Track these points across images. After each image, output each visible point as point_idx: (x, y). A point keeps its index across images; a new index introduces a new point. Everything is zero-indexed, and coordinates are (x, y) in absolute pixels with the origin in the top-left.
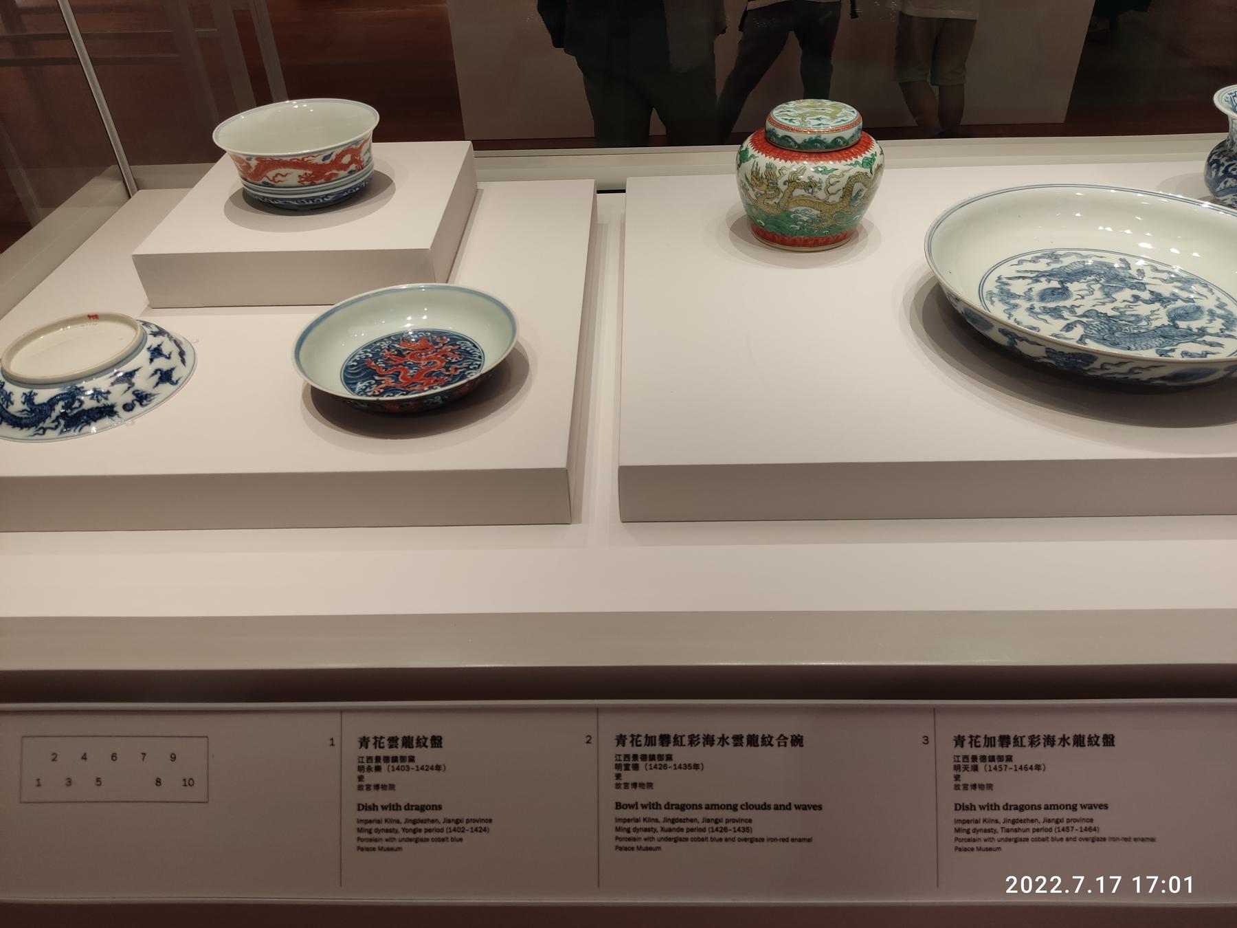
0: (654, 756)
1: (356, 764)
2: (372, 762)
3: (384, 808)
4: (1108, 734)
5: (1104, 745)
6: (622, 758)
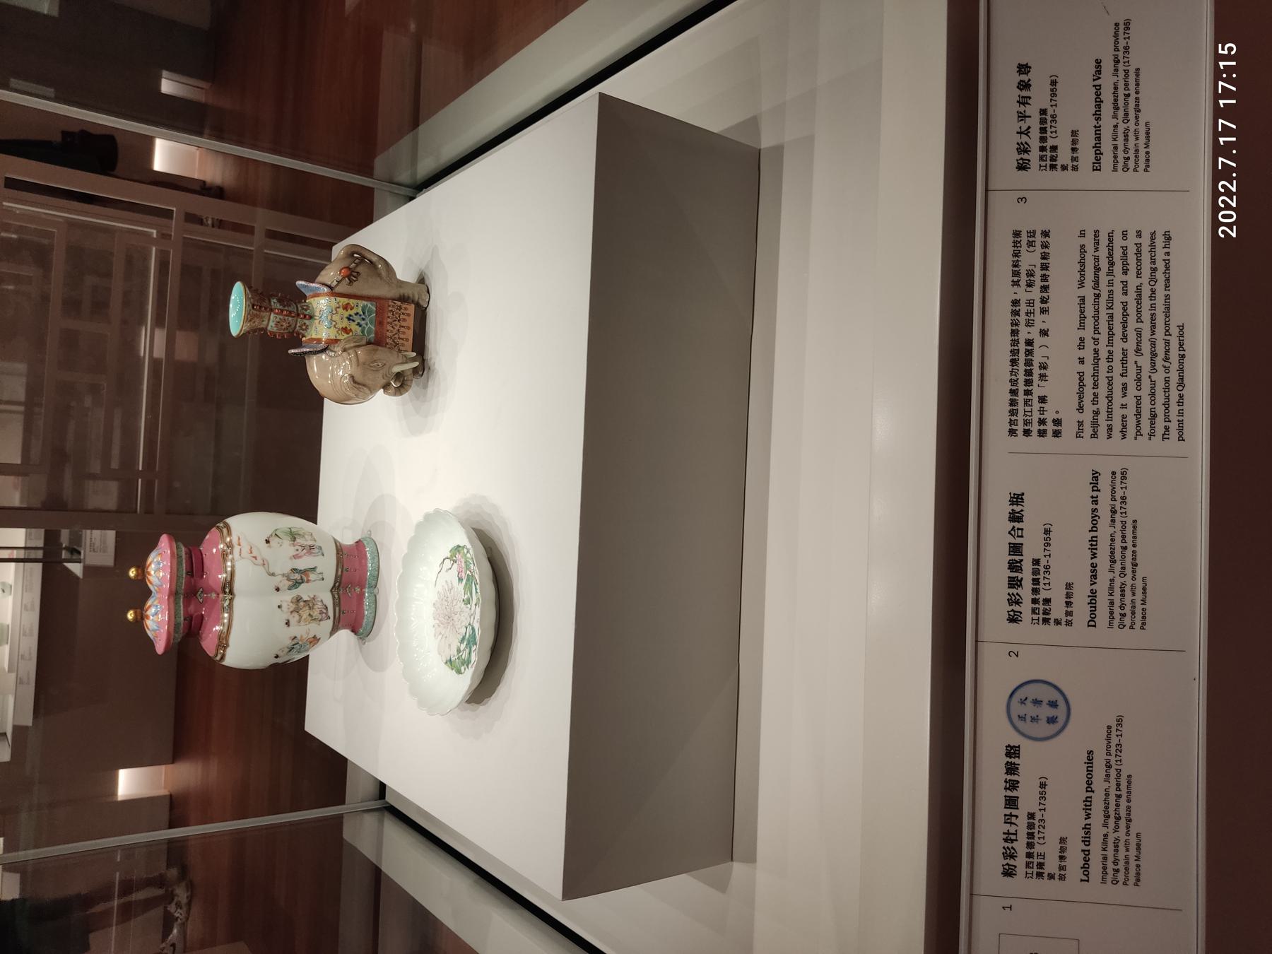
3: (1088, 816)
4: (1016, 165)
5: (1019, 757)
6: (1035, 617)
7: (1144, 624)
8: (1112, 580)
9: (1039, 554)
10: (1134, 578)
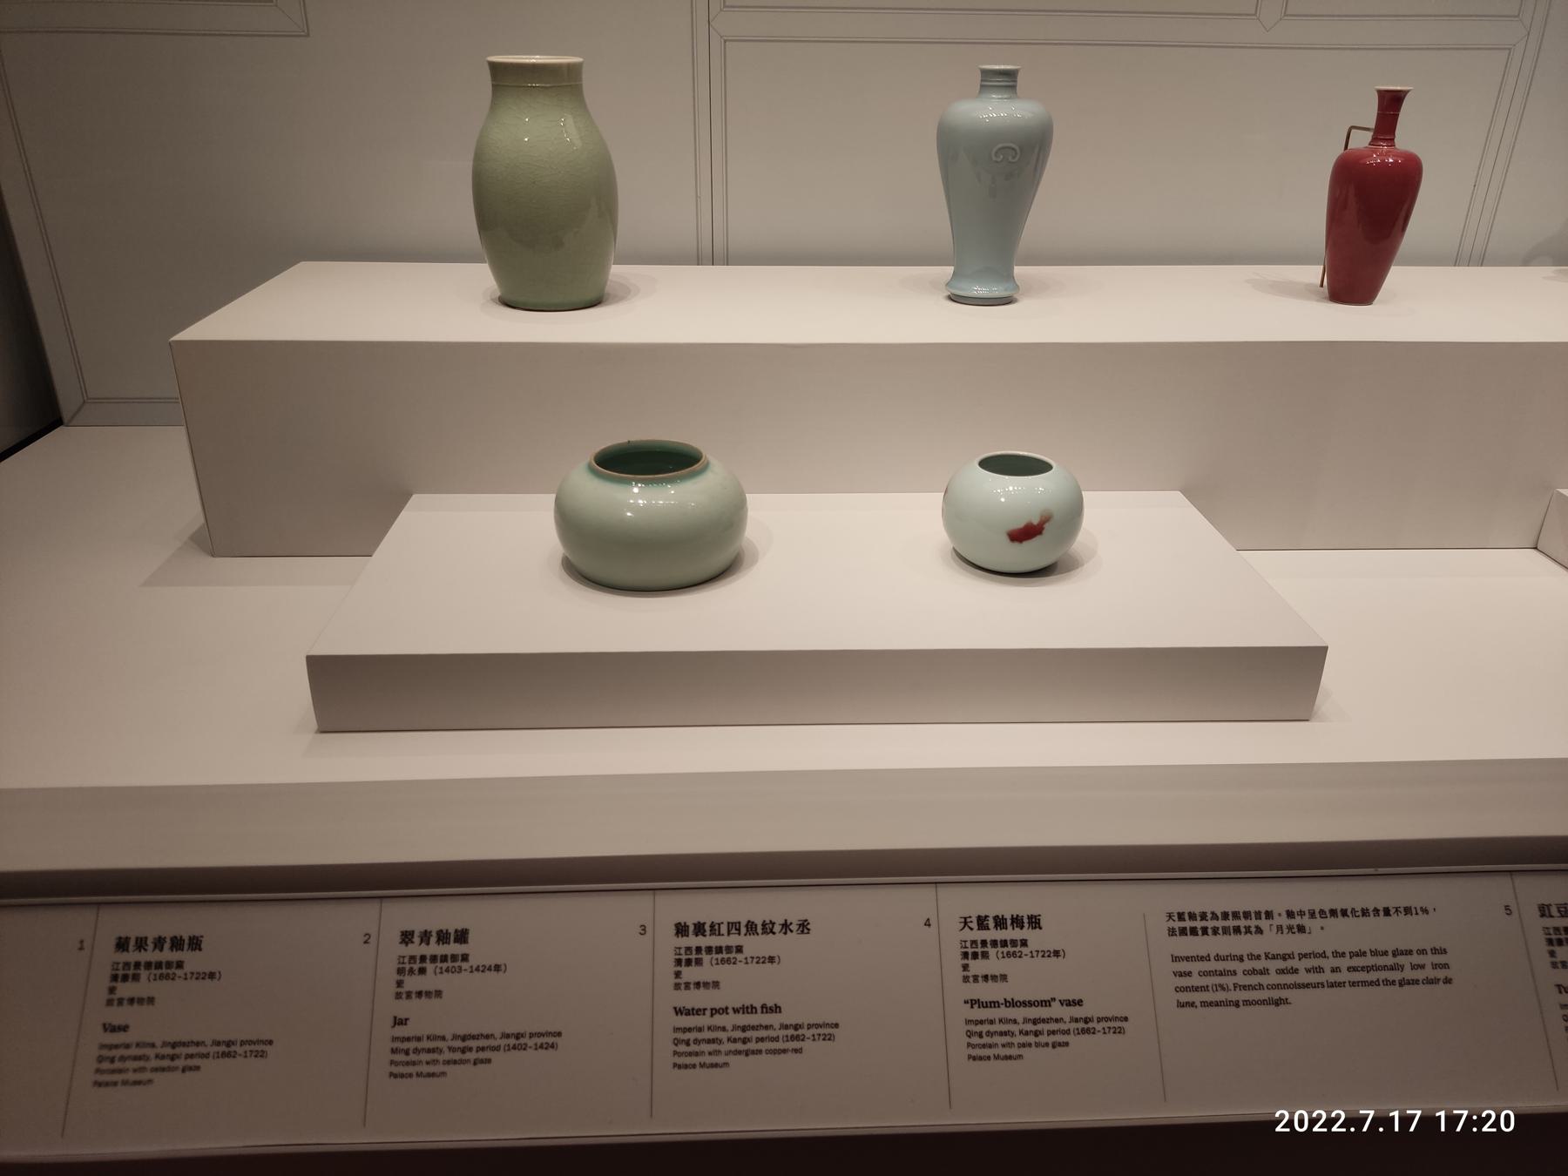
0: (721, 947)
1: (395, 966)
2: (415, 963)
6: (683, 951)
7: (680, 1067)
8: (724, 1029)
9: (747, 952)
10: (728, 1053)
